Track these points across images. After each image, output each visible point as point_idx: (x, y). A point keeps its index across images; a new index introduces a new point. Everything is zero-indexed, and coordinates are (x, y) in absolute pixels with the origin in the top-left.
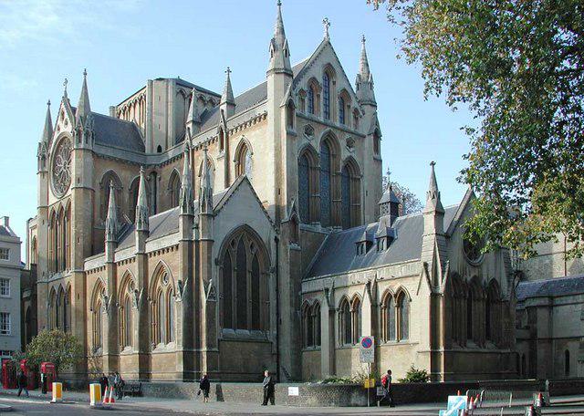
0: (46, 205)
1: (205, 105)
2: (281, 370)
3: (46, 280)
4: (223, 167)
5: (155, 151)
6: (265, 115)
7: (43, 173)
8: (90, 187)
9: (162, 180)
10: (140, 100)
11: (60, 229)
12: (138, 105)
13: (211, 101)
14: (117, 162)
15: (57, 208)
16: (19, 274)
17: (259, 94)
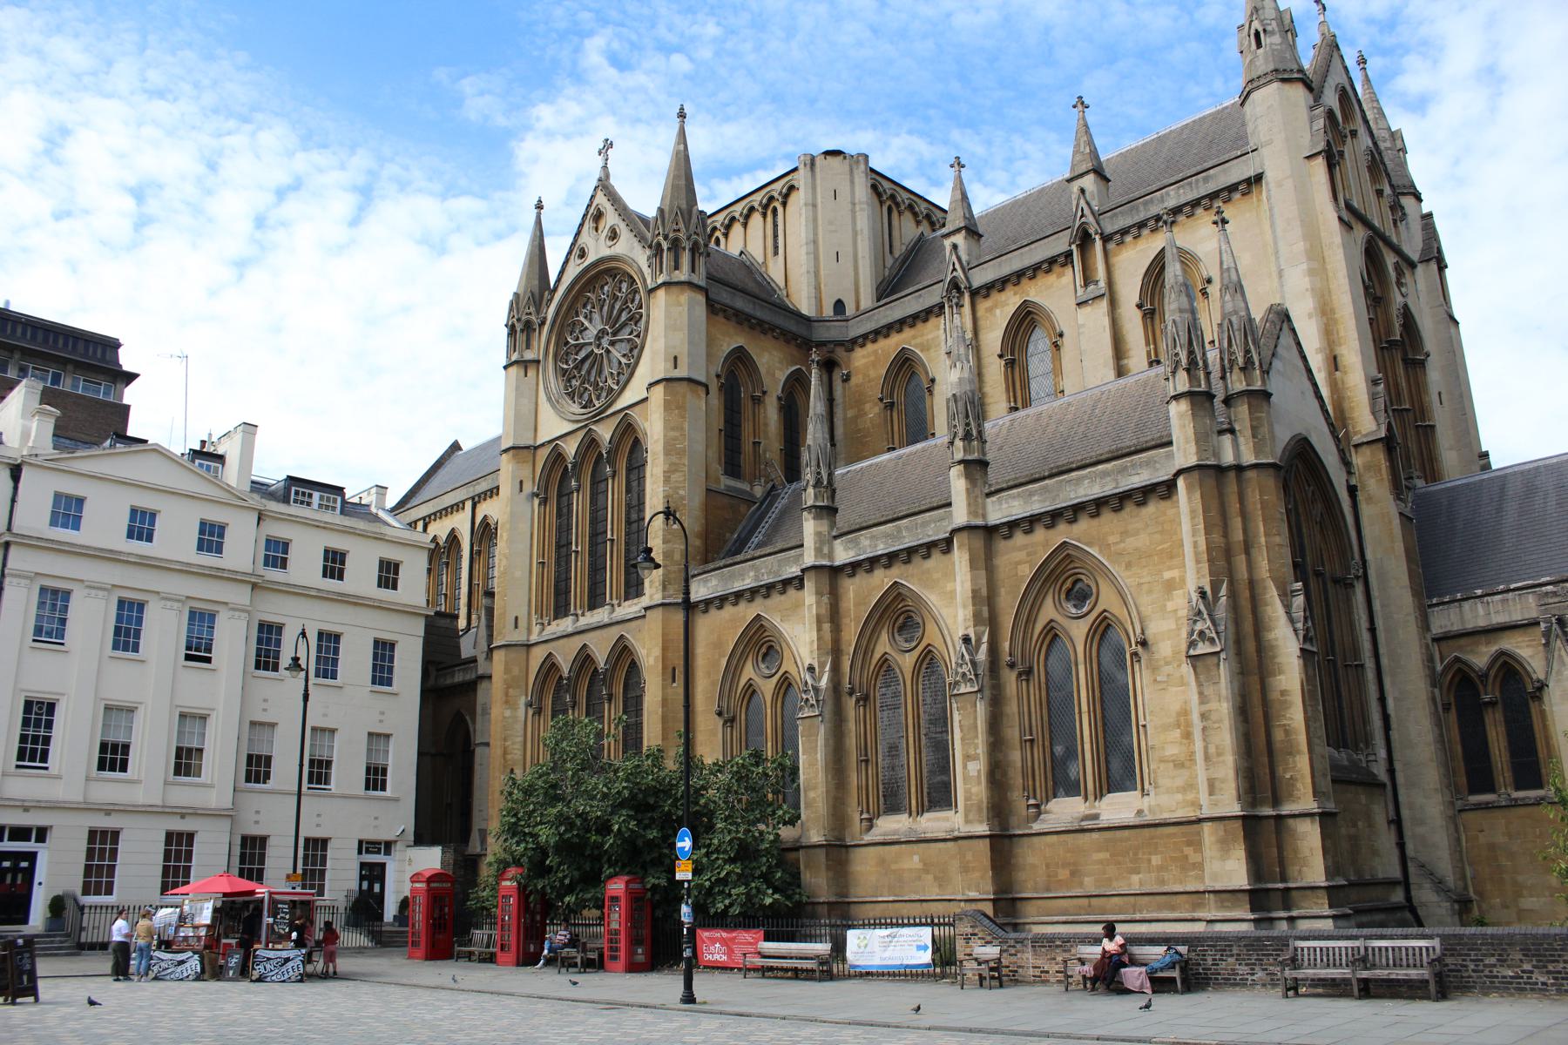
0: (531, 443)
1: (918, 223)
2: (1412, 869)
4: (1106, 321)
5: (828, 311)
6: (1258, 178)
7: (519, 364)
8: (703, 379)
9: (854, 381)
10: (766, 207)
11: (580, 504)
12: (756, 219)
13: (928, 217)
14: (752, 327)
15: (570, 448)
16: (419, 628)
17: (1225, 135)
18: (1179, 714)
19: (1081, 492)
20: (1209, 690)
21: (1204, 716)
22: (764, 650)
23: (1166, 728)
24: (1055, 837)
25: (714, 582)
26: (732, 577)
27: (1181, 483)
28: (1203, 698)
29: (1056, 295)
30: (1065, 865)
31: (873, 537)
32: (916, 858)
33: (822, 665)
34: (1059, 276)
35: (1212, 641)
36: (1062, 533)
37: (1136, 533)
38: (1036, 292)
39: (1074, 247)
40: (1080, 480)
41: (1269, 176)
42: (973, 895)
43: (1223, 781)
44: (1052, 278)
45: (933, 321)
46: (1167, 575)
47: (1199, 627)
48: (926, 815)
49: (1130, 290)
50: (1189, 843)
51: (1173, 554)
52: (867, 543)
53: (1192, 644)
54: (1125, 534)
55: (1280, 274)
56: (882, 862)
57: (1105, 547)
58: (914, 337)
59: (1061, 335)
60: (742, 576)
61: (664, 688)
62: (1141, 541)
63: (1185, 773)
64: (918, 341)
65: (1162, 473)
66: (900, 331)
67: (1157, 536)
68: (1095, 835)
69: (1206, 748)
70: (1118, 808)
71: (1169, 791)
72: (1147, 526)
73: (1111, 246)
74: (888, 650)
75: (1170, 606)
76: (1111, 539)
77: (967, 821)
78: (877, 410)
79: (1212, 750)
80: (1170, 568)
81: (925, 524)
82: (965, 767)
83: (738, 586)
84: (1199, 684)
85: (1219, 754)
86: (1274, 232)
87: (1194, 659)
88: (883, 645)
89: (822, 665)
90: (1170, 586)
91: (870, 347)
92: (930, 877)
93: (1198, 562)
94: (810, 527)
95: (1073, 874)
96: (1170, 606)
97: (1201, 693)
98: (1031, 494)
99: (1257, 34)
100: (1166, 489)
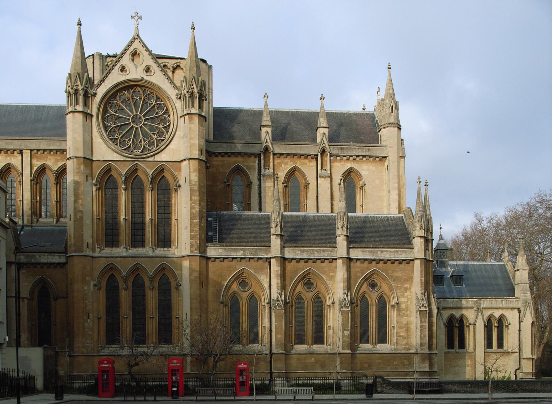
3: (91, 254)
9: (211, 170)
18: (405, 324)
19: (383, 255)
20: (423, 320)
21: (421, 326)
22: (241, 281)
23: (401, 328)
24: (364, 355)
25: (220, 251)
26: (230, 251)
27: (417, 262)
28: (421, 322)
29: (309, 169)
30: (367, 363)
31: (301, 251)
32: (313, 359)
33: (282, 292)
34: (310, 161)
35: (425, 307)
36: (373, 267)
37: (397, 272)
38: (299, 163)
39: (319, 154)
40: (382, 252)
41: (390, 158)
42: (344, 371)
43: (425, 344)
44: (307, 161)
45: (252, 158)
46: (406, 286)
47: (422, 302)
48: (314, 346)
49: (338, 177)
50: (405, 359)
51: (410, 279)
52: (299, 252)
53: (420, 307)
54: (394, 271)
55: (389, 192)
56: (299, 359)
57: (387, 273)
58: (244, 162)
59: (309, 184)
60: (236, 251)
61: (200, 290)
62: (399, 274)
63: (406, 340)
64: (246, 164)
65: (409, 256)
66: (236, 156)
67: (404, 274)
68: (377, 355)
69: (421, 335)
70: (382, 347)
71: (401, 345)
72: (401, 270)
73: (332, 158)
74: (302, 290)
75: (406, 294)
76: (390, 272)
77: (343, 349)
78: (223, 186)
79: (422, 335)
80: (407, 284)
81: (324, 251)
82: (343, 332)
83: (233, 255)
84: (421, 318)
85: (424, 337)
86: (389, 177)
87: (420, 311)
88: (300, 288)
89: (282, 292)
90: (406, 289)
91: (220, 158)
92: (318, 365)
93: (421, 285)
94: (276, 242)
95: (369, 366)
96: (406, 294)
97: (421, 320)
98: (365, 251)
99: (392, 107)
100: (410, 261)
